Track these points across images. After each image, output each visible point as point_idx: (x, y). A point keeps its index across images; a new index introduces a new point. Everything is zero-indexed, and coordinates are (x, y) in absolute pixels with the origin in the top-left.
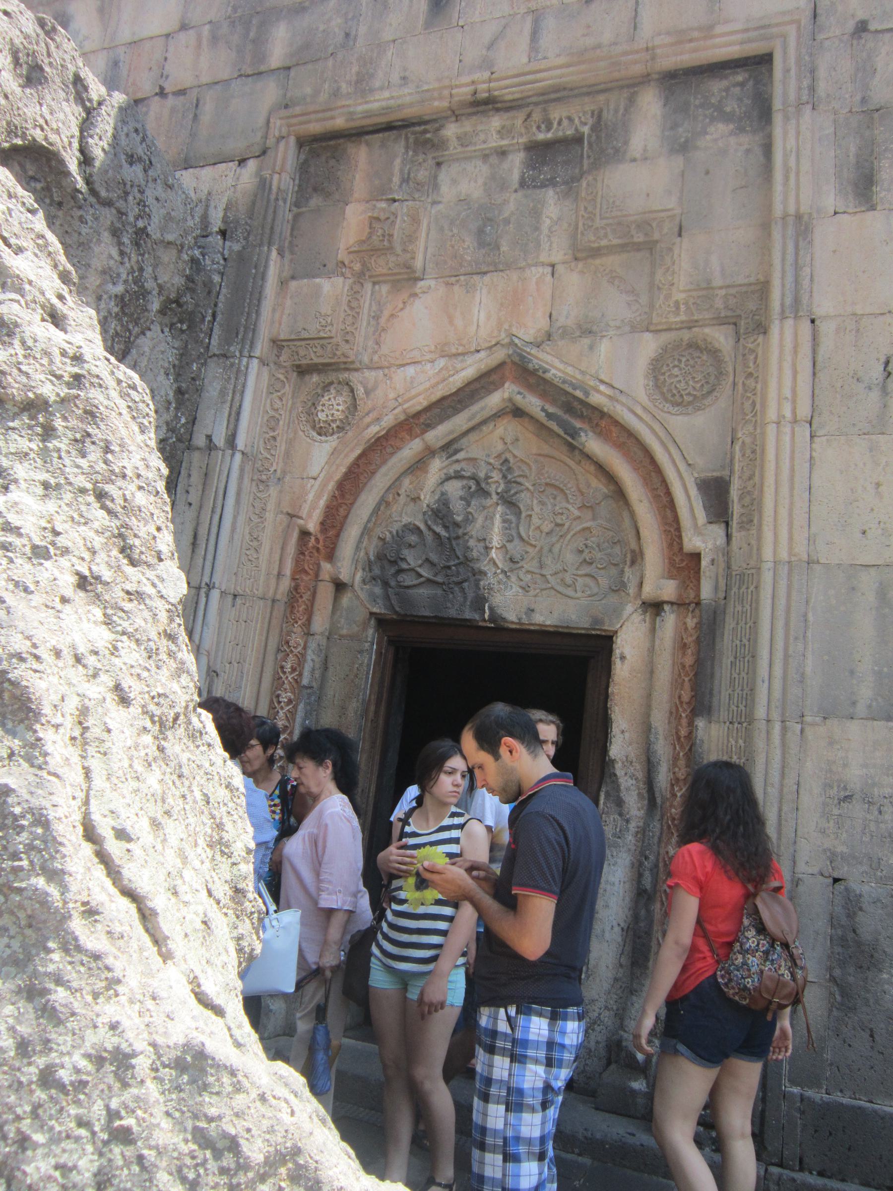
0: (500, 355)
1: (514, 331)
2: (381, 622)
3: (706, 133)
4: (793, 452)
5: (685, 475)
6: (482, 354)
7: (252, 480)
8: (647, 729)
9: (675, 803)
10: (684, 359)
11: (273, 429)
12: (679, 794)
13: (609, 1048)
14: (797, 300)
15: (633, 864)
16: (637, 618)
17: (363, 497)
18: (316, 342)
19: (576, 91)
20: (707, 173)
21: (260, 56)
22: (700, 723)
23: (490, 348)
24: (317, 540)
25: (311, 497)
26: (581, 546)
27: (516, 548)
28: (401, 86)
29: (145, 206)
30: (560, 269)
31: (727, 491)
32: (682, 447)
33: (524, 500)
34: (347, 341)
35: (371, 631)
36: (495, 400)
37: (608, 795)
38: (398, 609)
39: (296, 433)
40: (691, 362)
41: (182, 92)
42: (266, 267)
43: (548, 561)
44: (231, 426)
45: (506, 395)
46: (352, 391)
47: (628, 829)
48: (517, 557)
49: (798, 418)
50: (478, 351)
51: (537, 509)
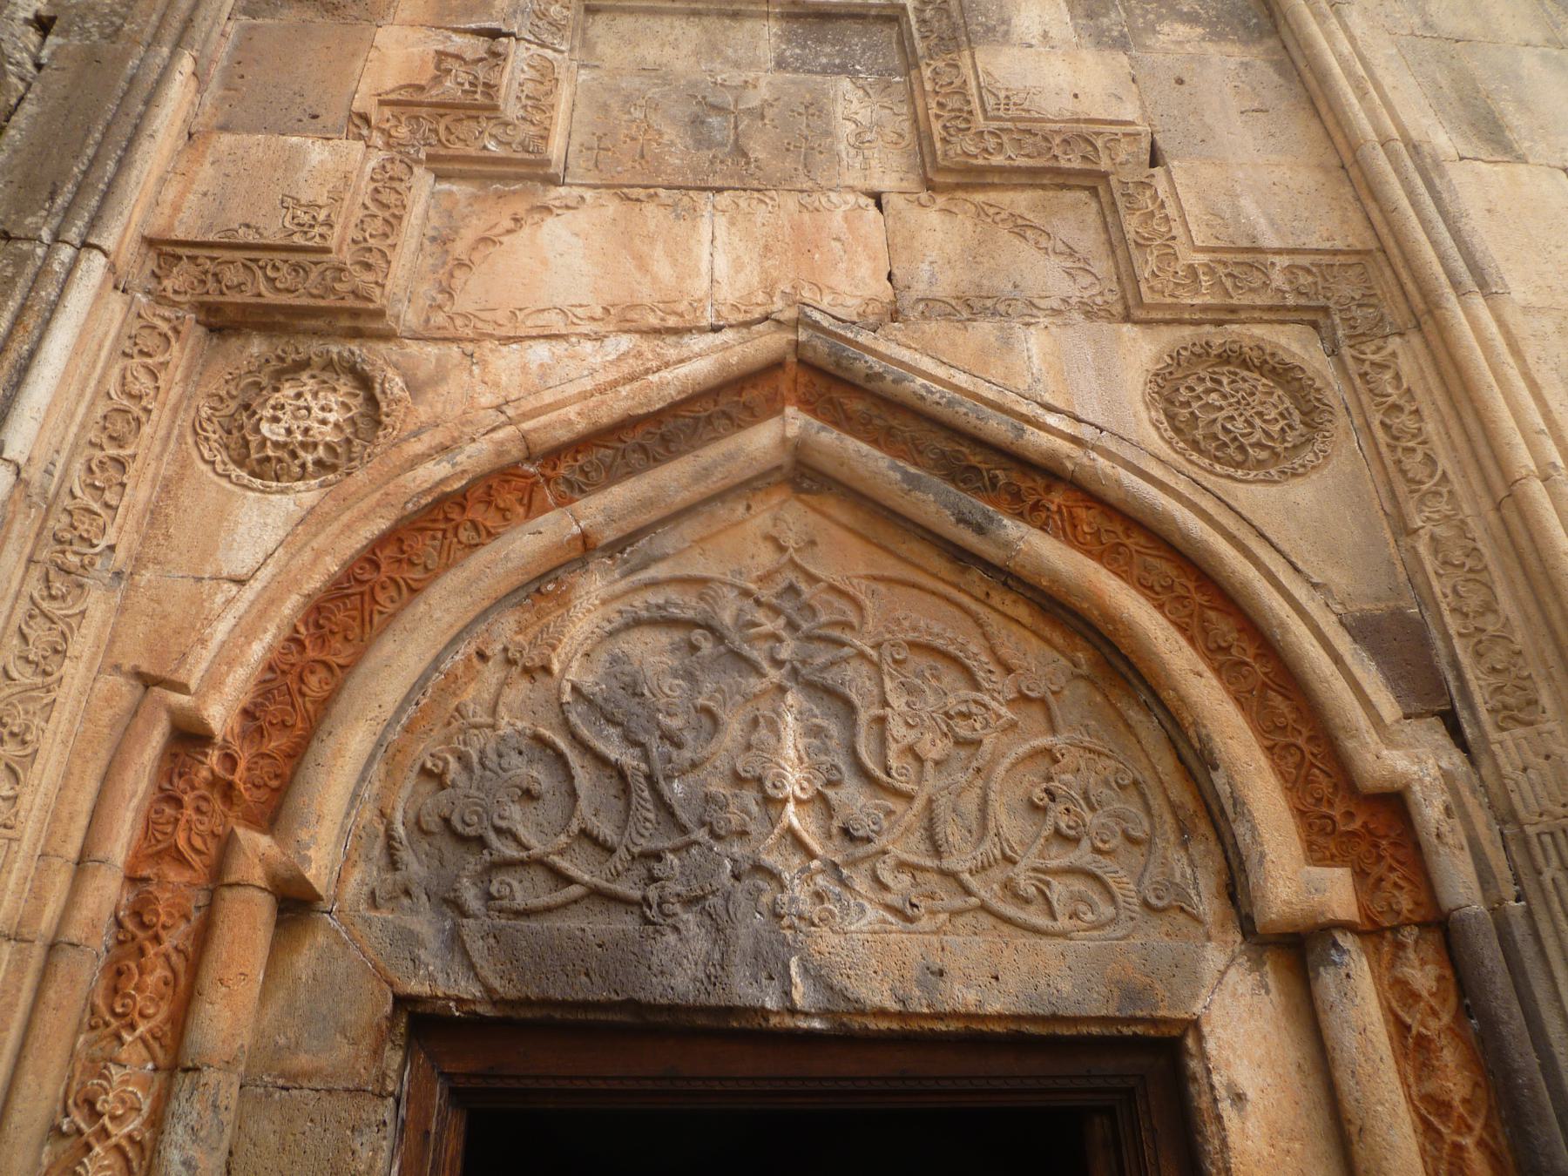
1: (807, 295)
3: (1155, 32)
6: (728, 335)
7: (30, 561)
16: (1241, 980)
17: (388, 647)
18: (278, 257)
23: (747, 324)
24: (230, 760)
25: (221, 630)
26: (1038, 794)
27: (853, 799)
30: (894, 201)
32: (1285, 547)
33: (856, 681)
34: (368, 267)
35: (393, 1058)
36: (761, 440)
38: (496, 983)
39: (185, 464)
43: (951, 832)
45: (792, 431)
46: (364, 381)
50: (716, 329)
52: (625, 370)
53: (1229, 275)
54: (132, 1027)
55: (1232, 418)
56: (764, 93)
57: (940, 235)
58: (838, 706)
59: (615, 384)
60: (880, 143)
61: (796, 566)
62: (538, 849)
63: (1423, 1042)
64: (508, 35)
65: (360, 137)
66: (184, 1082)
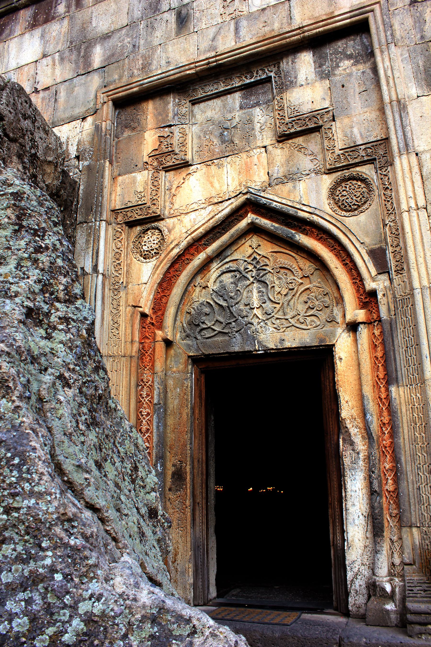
0: (242, 199)
2: (195, 360)
5: (360, 249)
6: (232, 200)
8: (362, 397)
9: (385, 438)
10: (348, 186)
12: (386, 432)
14: (407, 145)
15: (365, 478)
19: (264, 56)
20: (343, 86)
22: (393, 389)
23: (236, 196)
24: (152, 318)
27: (268, 306)
28: (167, 66)
29: (35, 141)
30: (270, 148)
31: (385, 254)
33: (268, 278)
34: (154, 204)
36: (243, 224)
37: (344, 440)
38: (204, 352)
40: (353, 187)
42: (104, 171)
43: (288, 310)
44: (94, 261)
45: (249, 221)
46: (161, 231)
47: (359, 458)
48: (270, 311)
49: (419, 207)
50: (230, 199)
51: (277, 282)
52: (211, 216)
53: (348, 155)
54: (146, 368)
55: (348, 198)
56: (237, 119)
57: (280, 157)
58: (265, 285)
59: (209, 220)
60: (266, 128)
61: (256, 253)
62: (209, 325)
63: (376, 345)
64: (173, 125)
65: (147, 169)
66: (155, 375)
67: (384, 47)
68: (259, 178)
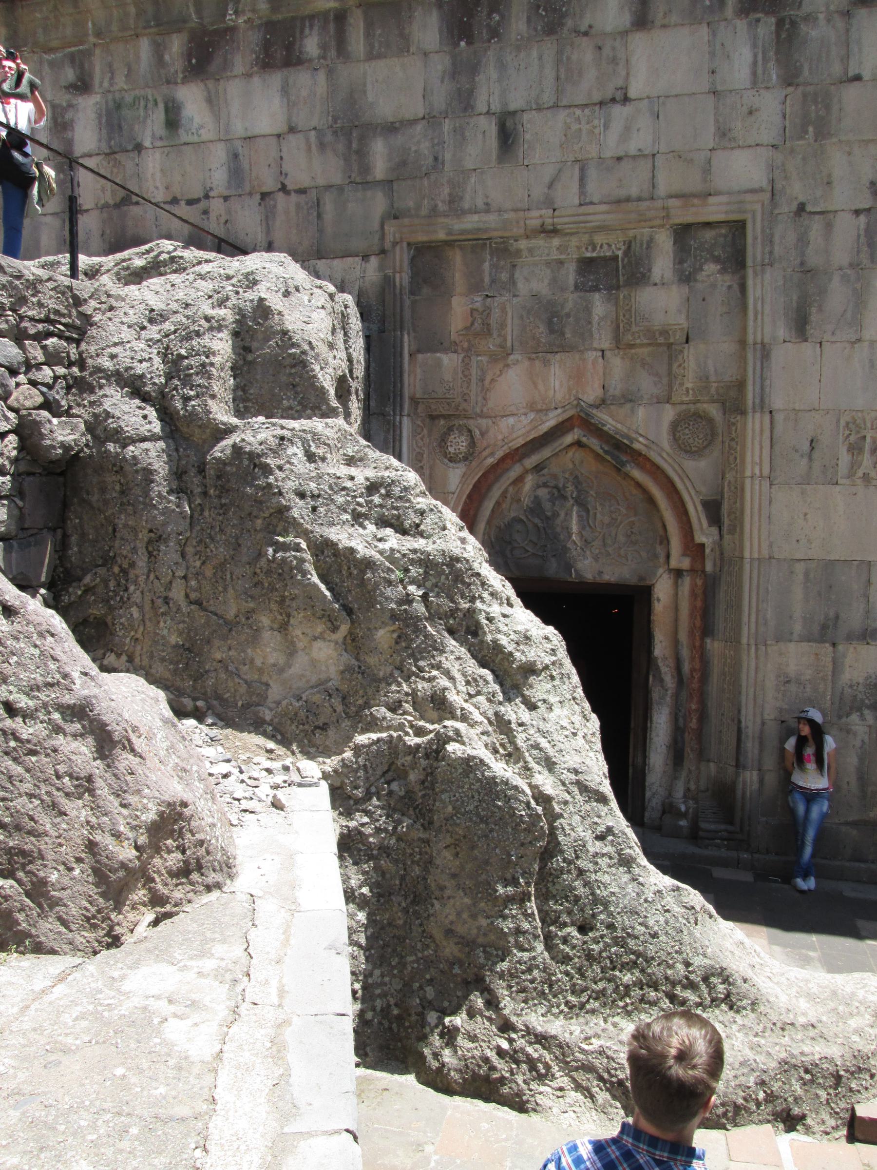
1: (580, 396)
3: (702, 270)
4: (760, 495)
6: (559, 411)
11: (420, 461)
13: (663, 805)
14: (762, 400)
16: (666, 576)
20: (704, 300)
21: (366, 169)
22: (708, 641)
27: (587, 533)
36: (569, 439)
41: (302, 191)
43: (609, 541)
45: (576, 437)
46: (470, 431)
51: (599, 508)
67: (759, 268)
68: (591, 394)
